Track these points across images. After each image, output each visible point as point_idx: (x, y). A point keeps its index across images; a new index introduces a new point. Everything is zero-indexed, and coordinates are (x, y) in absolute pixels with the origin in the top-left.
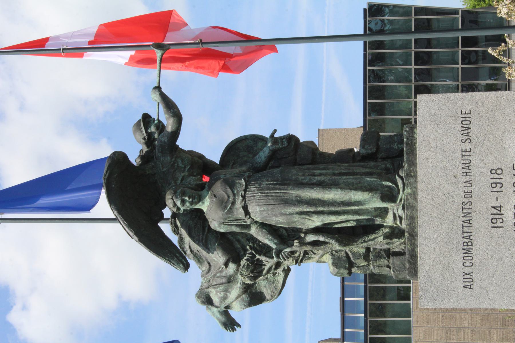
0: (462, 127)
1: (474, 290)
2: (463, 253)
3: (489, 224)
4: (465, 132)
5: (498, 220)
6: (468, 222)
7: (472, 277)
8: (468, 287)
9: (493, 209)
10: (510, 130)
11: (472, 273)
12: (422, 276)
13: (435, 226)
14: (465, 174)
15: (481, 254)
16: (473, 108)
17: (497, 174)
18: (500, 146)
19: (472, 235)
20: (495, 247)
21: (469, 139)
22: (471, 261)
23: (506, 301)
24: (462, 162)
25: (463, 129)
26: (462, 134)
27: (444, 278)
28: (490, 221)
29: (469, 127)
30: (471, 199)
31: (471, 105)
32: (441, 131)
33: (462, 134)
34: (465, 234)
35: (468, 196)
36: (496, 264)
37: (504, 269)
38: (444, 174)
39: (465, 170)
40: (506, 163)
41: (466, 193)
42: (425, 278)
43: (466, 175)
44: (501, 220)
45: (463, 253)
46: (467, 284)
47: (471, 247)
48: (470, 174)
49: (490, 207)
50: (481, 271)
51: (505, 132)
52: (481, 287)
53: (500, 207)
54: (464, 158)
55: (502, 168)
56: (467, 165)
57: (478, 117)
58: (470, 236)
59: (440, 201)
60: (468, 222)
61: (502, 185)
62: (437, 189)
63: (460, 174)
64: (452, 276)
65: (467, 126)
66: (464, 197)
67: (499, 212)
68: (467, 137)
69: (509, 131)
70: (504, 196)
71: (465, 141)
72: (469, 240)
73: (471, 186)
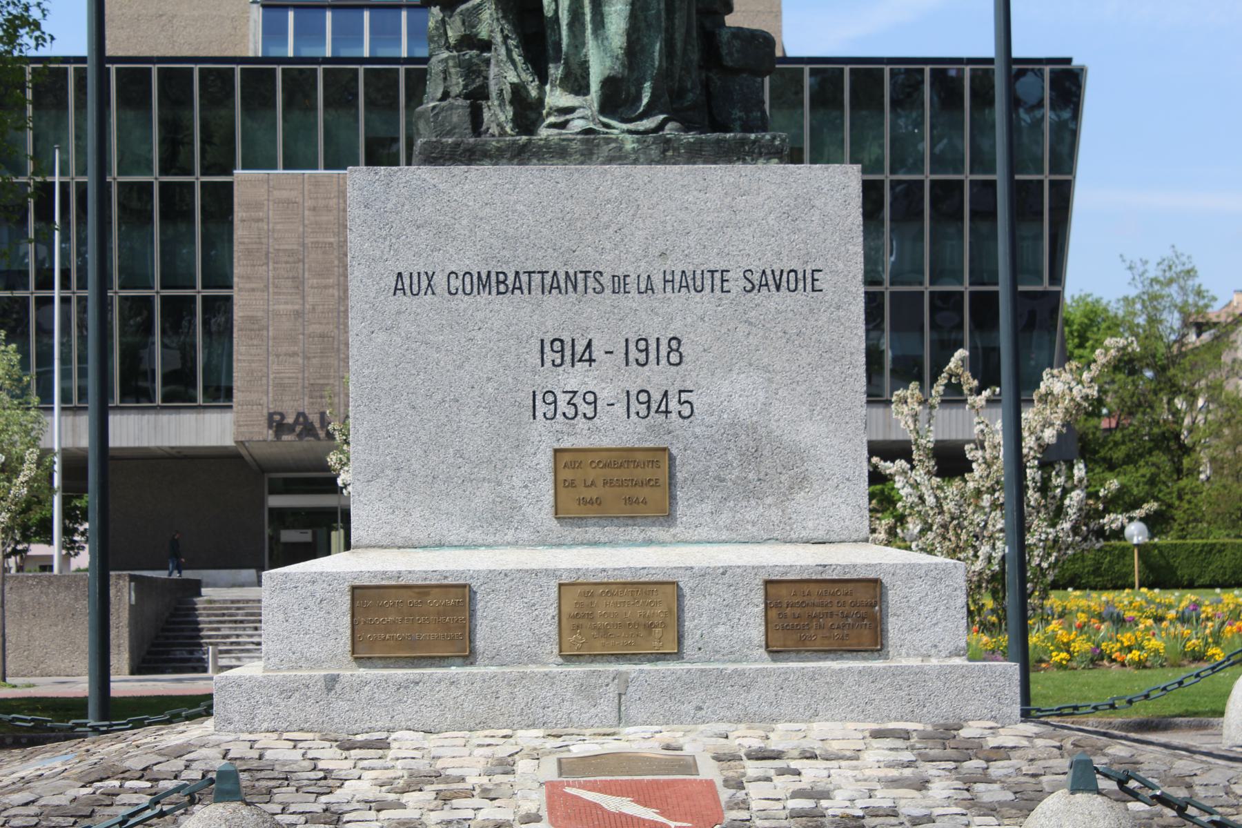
0: (782, 272)
1: (392, 298)
2: (479, 273)
3: (549, 334)
4: (770, 277)
5: (559, 355)
6: (555, 285)
7: (423, 292)
8: (400, 283)
9: (585, 342)
10: (772, 382)
11: (433, 293)
12: (423, 176)
13: (543, 207)
14: (669, 277)
15: (480, 315)
16: (826, 298)
17: (669, 353)
18: (734, 361)
19: (522, 293)
20: (495, 348)
21: (753, 288)
22: (460, 291)
23: (366, 372)
24: (699, 272)
25: (777, 274)
26: (764, 272)
27: (418, 227)
28: (557, 336)
29: (782, 288)
30: (608, 291)
31: (834, 292)
32: (771, 223)
33: (764, 272)
34: (524, 278)
35: (616, 285)
36: (455, 350)
37: (442, 368)
38: (670, 229)
39: (677, 278)
40: (694, 374)
41: (624, 280)
42: (419, 183)
43: (666, 281)
44: (558, 361)
45: (479, 273)
46: (407, 282)
47: (494, 291)
48: (669, 289)
49: (589, 337)
50: (437, 314)
51: (769, 372)
52: (399, 313)
53: (591, 360)
54: (707, 275)
55: (683, 365)
56: (691, 283)
57: (806, 309)
58: (520, 288)
59: (605, 219)
60: (555, 285)
61: (643, 365)
62: (632, 212)
63: (668, 265)
64: (424, 247)
65: (784, 284)
66: (614, 276)
67: (577, 357)
68: (756, 283)
69: (770, 381)
70: (616, 368)
71: (747, 279)
72: (511, 287)
73: (639, 293)
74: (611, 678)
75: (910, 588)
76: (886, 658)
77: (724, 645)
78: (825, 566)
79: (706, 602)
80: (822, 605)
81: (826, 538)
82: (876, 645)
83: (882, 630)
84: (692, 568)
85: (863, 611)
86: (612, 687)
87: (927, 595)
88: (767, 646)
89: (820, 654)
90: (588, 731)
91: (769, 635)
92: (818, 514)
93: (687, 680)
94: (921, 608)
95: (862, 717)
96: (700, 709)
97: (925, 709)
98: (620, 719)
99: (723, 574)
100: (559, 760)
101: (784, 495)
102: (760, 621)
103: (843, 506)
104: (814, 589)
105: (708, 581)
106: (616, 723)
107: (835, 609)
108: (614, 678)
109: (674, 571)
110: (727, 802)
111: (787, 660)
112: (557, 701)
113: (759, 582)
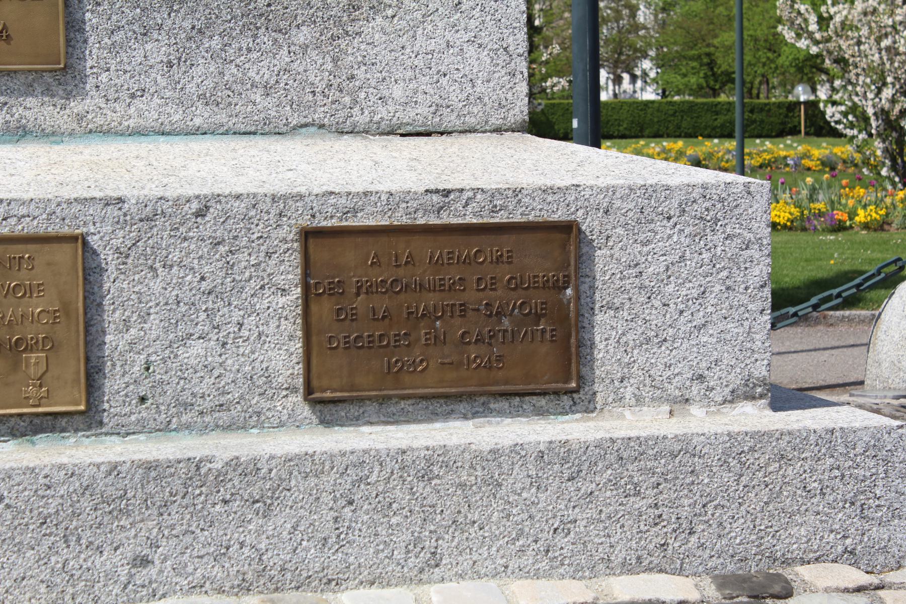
75: (645, 244)
76: (589, 407)
77: (203, 388)
78: (447, 193)
79: (157, 286)
80: (440, 287)
81: (430, 125)
82: (567, 380)
83: (580, 344)
84: (120, 200)
85: (537, 299)
87: (682, 258)
88: (309, 390)
89: (436, 405)
91: (314, 361)
92: (414, 68)
93: (110, 491)
94: (670, 288)
95: (544, 565)
96: (145, 562)
97: (693, 539)
99: (200, 214)
101: (339, 23)
102: (293, 327)
103: (471, 51)
104: (423, 248)
105: (161, 231)
107: (470, 296)
109: (76, 208)
111: (356, 421)
113: (288, 232)
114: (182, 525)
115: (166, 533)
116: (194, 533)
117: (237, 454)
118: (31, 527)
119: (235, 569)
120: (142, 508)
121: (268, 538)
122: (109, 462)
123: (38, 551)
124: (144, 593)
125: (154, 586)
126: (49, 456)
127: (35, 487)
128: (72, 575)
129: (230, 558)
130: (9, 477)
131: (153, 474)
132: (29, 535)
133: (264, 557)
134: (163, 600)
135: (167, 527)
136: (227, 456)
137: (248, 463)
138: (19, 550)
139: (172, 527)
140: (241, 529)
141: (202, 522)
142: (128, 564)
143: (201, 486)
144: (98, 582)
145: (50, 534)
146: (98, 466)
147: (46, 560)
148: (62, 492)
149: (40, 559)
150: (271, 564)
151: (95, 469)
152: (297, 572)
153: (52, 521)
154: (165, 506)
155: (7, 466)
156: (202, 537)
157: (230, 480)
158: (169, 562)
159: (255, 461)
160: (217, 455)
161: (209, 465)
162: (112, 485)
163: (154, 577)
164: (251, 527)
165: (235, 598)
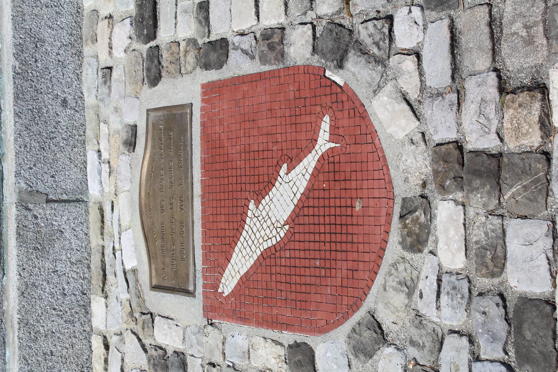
74: (26, 213)
86: (38, 211)
90: (95, 241)
93: (28, 117)
96: (65, 101)
98: (78, 201)
100: (156, 288)
106: (83, 206)
108: (27, 209)
110: (264, 60)
112: (56, 279)
114: (47, 83)
115: (51, 91)
116: (51, 77)
117: (12, 54)
118: (45, 155)
119: (70, 58)
120: (38, 102)
121: (55, 41)
122: (14, 117)
123: (57, 151)
124: (80, 102)
125: (76, 97)
126: (10, 146)
127: (25, 153)
128: (70, 136)
129: (64, 60)
130: (20, 165)
131: (21, 96)
132: (49, 155)
133: (65, 43)
134: (84, 93)
135: (48, 90)
136: (12, 59)
137: (16, 49)
138: (56, 160)
139: (48, 88)
140: (50, 54)
141: (46, 73)
142: (65, 109)
143: (28, 72)
144: (74, 124)
145: (49, 146)
146: (16, 122)
147: (62, 148)
148: (28, 140)
149: (61, 151)
150: (68, 40)
151: (17, 124)
152: (73, 28)
153: (43, 145)
154: (37, 91)
155: (14, 165)
156: (53, 73)
157: (25, 58)
158: (65, 90)
159: (15, 45)
160: (12, 64)
161: (17, 68)
162: (25, 116)
163: (72, 97)
164: (49, 49)
165: (84, 59)
